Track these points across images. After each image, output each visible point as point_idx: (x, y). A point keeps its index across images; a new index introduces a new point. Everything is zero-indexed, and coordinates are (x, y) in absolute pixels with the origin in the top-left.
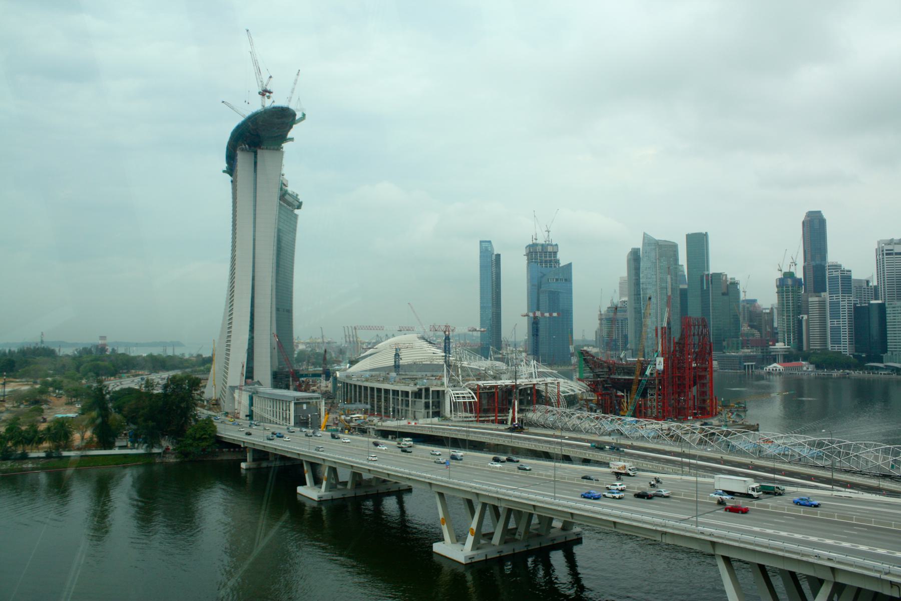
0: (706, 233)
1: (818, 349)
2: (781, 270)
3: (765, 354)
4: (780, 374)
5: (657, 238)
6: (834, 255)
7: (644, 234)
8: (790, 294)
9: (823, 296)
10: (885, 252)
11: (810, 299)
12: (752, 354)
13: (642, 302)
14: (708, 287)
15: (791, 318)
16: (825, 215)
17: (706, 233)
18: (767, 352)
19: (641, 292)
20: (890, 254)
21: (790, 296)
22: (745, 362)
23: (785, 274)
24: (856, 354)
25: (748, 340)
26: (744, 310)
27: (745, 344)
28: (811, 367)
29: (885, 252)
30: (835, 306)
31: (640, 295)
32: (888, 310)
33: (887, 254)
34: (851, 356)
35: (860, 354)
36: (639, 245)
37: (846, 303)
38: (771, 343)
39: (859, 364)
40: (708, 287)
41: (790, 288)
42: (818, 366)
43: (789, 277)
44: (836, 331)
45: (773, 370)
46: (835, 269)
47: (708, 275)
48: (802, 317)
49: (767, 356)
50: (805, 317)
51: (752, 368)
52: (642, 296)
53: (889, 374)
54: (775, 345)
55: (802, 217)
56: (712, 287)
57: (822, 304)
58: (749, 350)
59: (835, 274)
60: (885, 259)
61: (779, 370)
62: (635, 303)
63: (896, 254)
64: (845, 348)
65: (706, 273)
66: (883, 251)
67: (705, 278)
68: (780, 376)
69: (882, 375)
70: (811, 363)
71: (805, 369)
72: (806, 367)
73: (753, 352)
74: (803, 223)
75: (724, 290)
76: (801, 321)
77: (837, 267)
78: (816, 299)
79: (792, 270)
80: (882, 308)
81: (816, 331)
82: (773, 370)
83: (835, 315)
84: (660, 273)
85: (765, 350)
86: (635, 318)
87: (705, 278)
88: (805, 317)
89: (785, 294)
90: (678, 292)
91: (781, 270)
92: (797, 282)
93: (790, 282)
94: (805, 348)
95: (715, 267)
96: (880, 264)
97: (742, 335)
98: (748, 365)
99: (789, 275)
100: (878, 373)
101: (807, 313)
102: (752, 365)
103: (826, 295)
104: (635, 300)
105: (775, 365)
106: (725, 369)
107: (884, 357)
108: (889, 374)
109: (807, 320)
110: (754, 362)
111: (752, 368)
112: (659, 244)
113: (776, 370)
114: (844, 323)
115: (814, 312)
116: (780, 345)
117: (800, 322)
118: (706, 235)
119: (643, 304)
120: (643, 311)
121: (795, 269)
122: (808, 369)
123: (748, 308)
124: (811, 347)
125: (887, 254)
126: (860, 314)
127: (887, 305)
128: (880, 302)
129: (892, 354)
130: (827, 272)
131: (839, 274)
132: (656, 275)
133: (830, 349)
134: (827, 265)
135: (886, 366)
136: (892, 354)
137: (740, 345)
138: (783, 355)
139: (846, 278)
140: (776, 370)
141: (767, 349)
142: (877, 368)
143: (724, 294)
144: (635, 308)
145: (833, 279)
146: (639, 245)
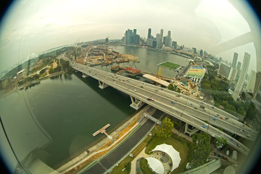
6: (152, 34)
30: (151, 40)
36: (127, 30)
37: (152, 40)
39: (153, 48)
44: (151, 43)
55: (148, 29)
57: (150, 40)
64: (152, 45)
77: (152, 36)
83: (151, 41)
95: (137, 34)
96: (157, 36)
103: (150, 39)
126: (154, 42)
139: (153, 37)
145: (151, 37)
146: (127, 30)
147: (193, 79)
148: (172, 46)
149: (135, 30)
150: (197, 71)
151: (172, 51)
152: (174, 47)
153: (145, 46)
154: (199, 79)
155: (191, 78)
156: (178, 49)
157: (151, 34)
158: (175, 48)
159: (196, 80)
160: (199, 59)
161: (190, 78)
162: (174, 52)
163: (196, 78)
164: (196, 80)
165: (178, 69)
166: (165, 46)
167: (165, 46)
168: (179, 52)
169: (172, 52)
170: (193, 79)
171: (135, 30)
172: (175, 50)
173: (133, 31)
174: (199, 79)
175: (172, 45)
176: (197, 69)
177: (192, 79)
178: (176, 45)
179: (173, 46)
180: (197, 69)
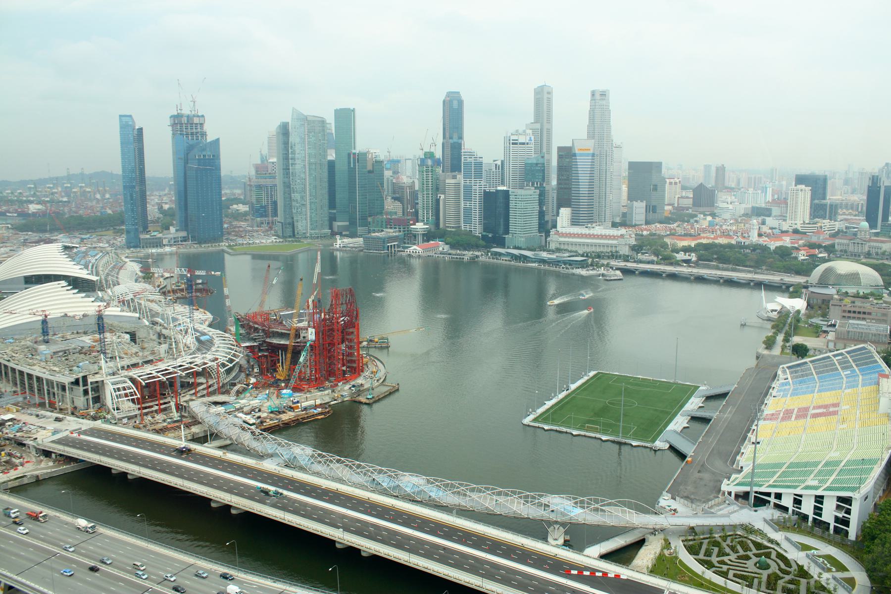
0: (354, 109)
1: (453, 227)
2: (422, 150)
3: (406, 232)
4: (419, 256)
5: (305, 114)
7: (293, 109)
8: (430, 173)
9: (458, 179)
10: (511, 142)
11: (447, 181)
12: (394, 234)
13: (291, 178)
14: (355, 165)
15: (430, 196)
16: (464, 97)
17: (354, 109)
18: (408, 231)
19: (290, 167)
20: (516, 144)
21: (430, 176)
22: (389, 243)
23: (426, 154)
24: (484, 233)
25: (391, 219)
26: (388, 183)
27: (389, 223)
28: (447, 248)
29: (511, 142)
30: (468, 189)
31: (289, 169)
32: (512, 198)
33: (513, 144)
34: (480, 235)
35: (488, 234)
38: (411, 222)
40: (355, 165)
41: (430, 168)
42: (453, 246)
43: (429, 158)
44: (468, 212)
45: (413, 252)
46: (469, 155)
47: (354, 154)
48: (440, 197)
49: (408, 234)
50: (442, 197)
51: (394, 248)
52: (291, 171)
53: (509, 261)
54: (415, 225)
56: (358, 166)
58: (392, 230)
59: (469, 160)
60: (511, 148)
61: (419, 252)
62: (284, 177)
63: (521, 144)
65: (354, 151)
66: (510, 140)
67: (352, 156)
68: (419, 258)
69: (503, 261)
70: (447, 244)
71: (441, 249)
72: (442, 247)
73: (396, 232)
74: (444, 102)
75: (370, 167)
76: (439, 199)
77: (471, 154)
78: (453, 181)
79: (432, 150)
80: (506, 194)
81: (451, 211)
82: (413, 252)
83: (468, 197)
84: (309, 148)
85: (406, 229)
86: (284, 193)
87: (352, 156)
88: (442, 197)
89: (425, 174)
90: (326, 167)
91: (422, 150)
92: (437, 162)
93: (430, 162)
94: (441, 226)
95: (360, 146)
97: (387, 214)
98: (391, 246)
99: (430, 155)
100: (500, 260)
101: (444, 193)
102: (394, 245)
103: (460, 177)
104: (284, 174)
105: (415, 247)
106: (370, 250)
107: (506, 239)
108: (509, 261)
109: (445, 199)
110: (396, 242)
111: (394, 248)
112: (308, 119)
113: (416, 252)
114: (476, 205)
115: (451, 192)
116: (420, 226)
117: (438, 201)
118: (354, 110)
119: (292, 179)
120: (292, 186)
121: (435, 149)
122: (443, 249)
123: (392, 180)
124: (447, 225)
125: (513, 144)
127: (510, 193)
128: (505, 188)
129: (513, 236)
130: (463, 157)
131: (472, 160)
132: (305, 150)
133: (463, 229)
134: (463, 151)
135: (507, 252)
136: (513, 236)
137: (384, 223)
138: (423, 234)
140: (416, 252)
141: (408, 228)
142: (500, 254)
143: (370, 172)
144: (284, 183)
145: (468, 165)
146: (288, 119)
147: (797, 502)
148: (632, 197)
149: (346, 117)
150: (829, 411)
151: (625, 251)
152: (639, 207)
153: (428, 236)
154: (848, 501)
155: (779, 496)
156: (680, 215)
157: (461, 138)
158: (651, 209)
159: (818, 511)
160: (854, 278)
161: (772, 499)
162: (647, 262)
163: (819, 499)
164: (818, 511)
165: (679, 422)
166: (575, 222)
167: (575, 222)
168: (686, 250)
169: (631, 265)
170: (797, 502)
171: (346, 117)
172: (658, 228)
173: (330, 119)
174: (840, 499)
175: (625, 188)
176: (828, 397)
177: (787, 502)
178: (655, 188)
179: (636, 204)
180: (828, 397)
